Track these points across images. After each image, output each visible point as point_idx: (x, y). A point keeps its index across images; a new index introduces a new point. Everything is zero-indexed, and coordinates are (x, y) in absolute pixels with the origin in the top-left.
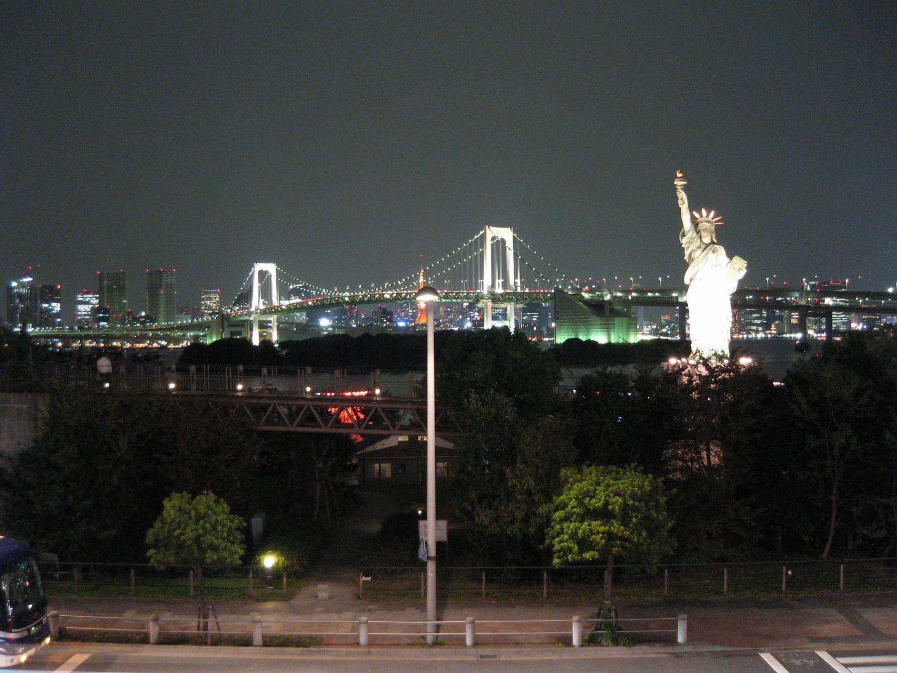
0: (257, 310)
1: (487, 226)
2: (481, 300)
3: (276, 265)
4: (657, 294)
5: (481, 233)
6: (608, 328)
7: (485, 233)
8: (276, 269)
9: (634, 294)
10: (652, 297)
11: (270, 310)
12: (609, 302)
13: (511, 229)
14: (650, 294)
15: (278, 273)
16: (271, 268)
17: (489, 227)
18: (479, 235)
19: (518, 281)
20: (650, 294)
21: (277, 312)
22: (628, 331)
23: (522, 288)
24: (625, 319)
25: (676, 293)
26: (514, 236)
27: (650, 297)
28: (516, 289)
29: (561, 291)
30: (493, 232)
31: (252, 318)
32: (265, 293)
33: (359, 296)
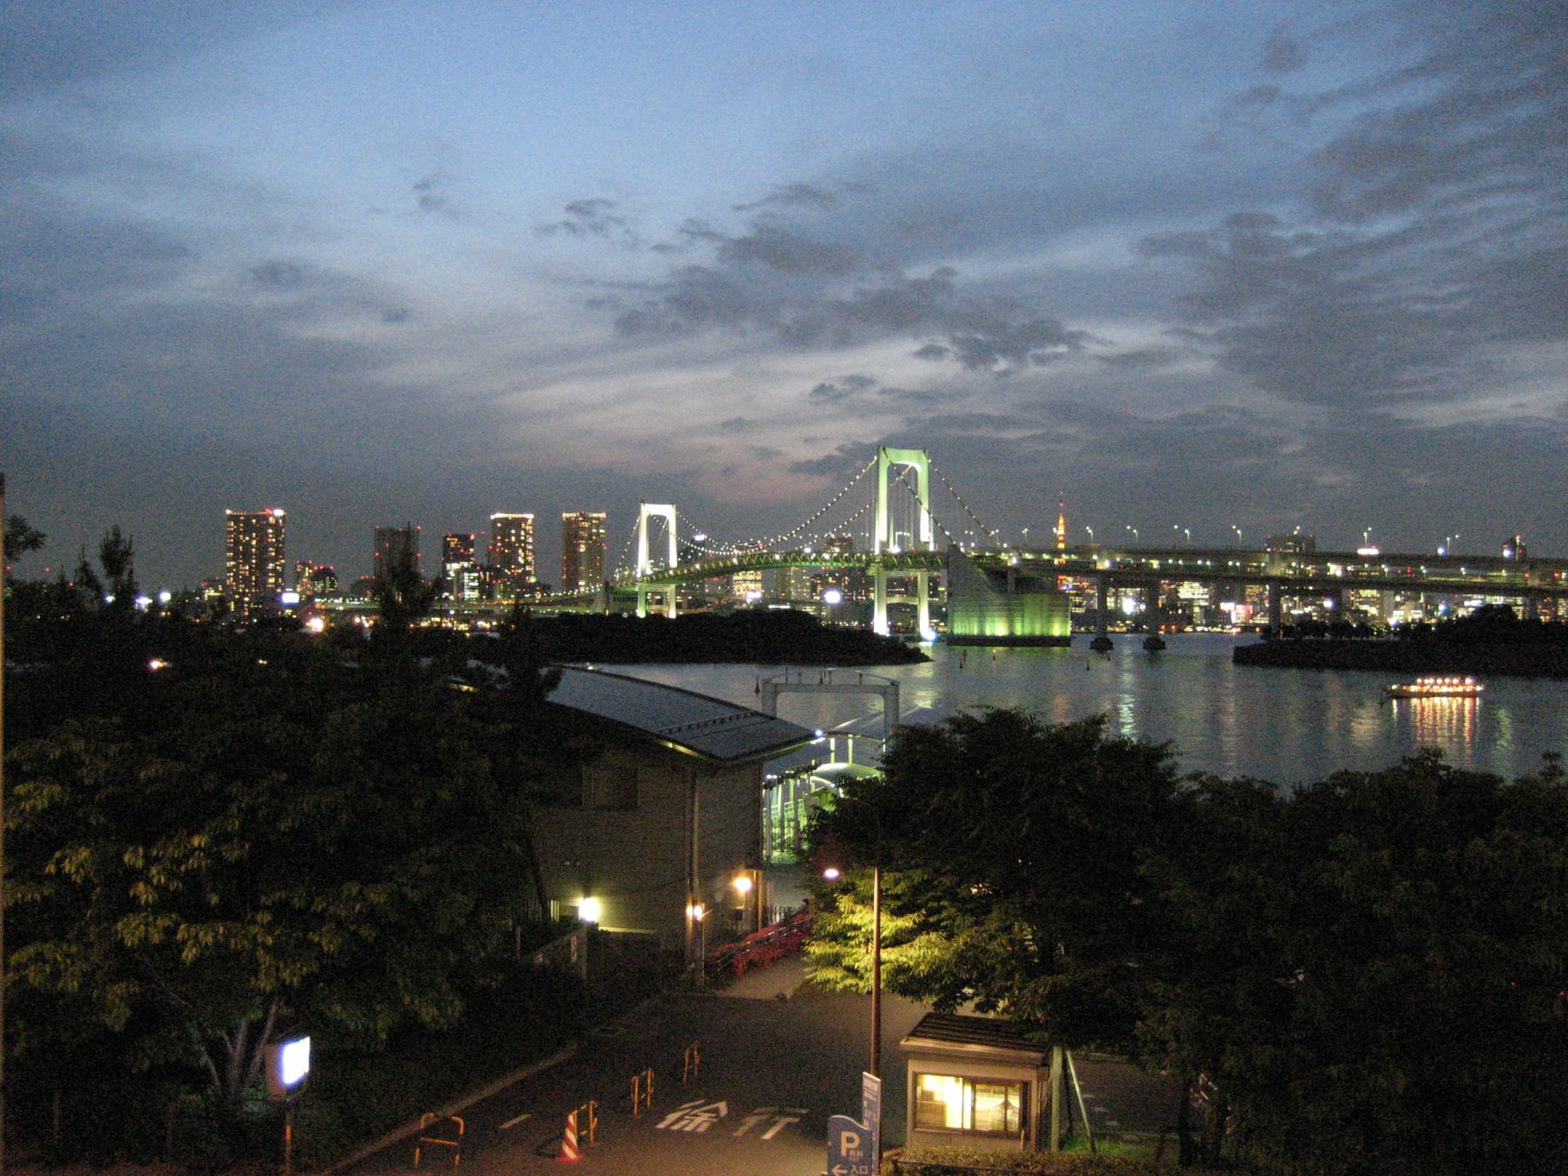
4: (1074, 557)
6: (1009, 610)
11: (660, 577)
15: (678, 520)
16: (668, 512)
22: (1051, 616)
24: (1046, 599)
31: (637, 589)
32: (658, 551)
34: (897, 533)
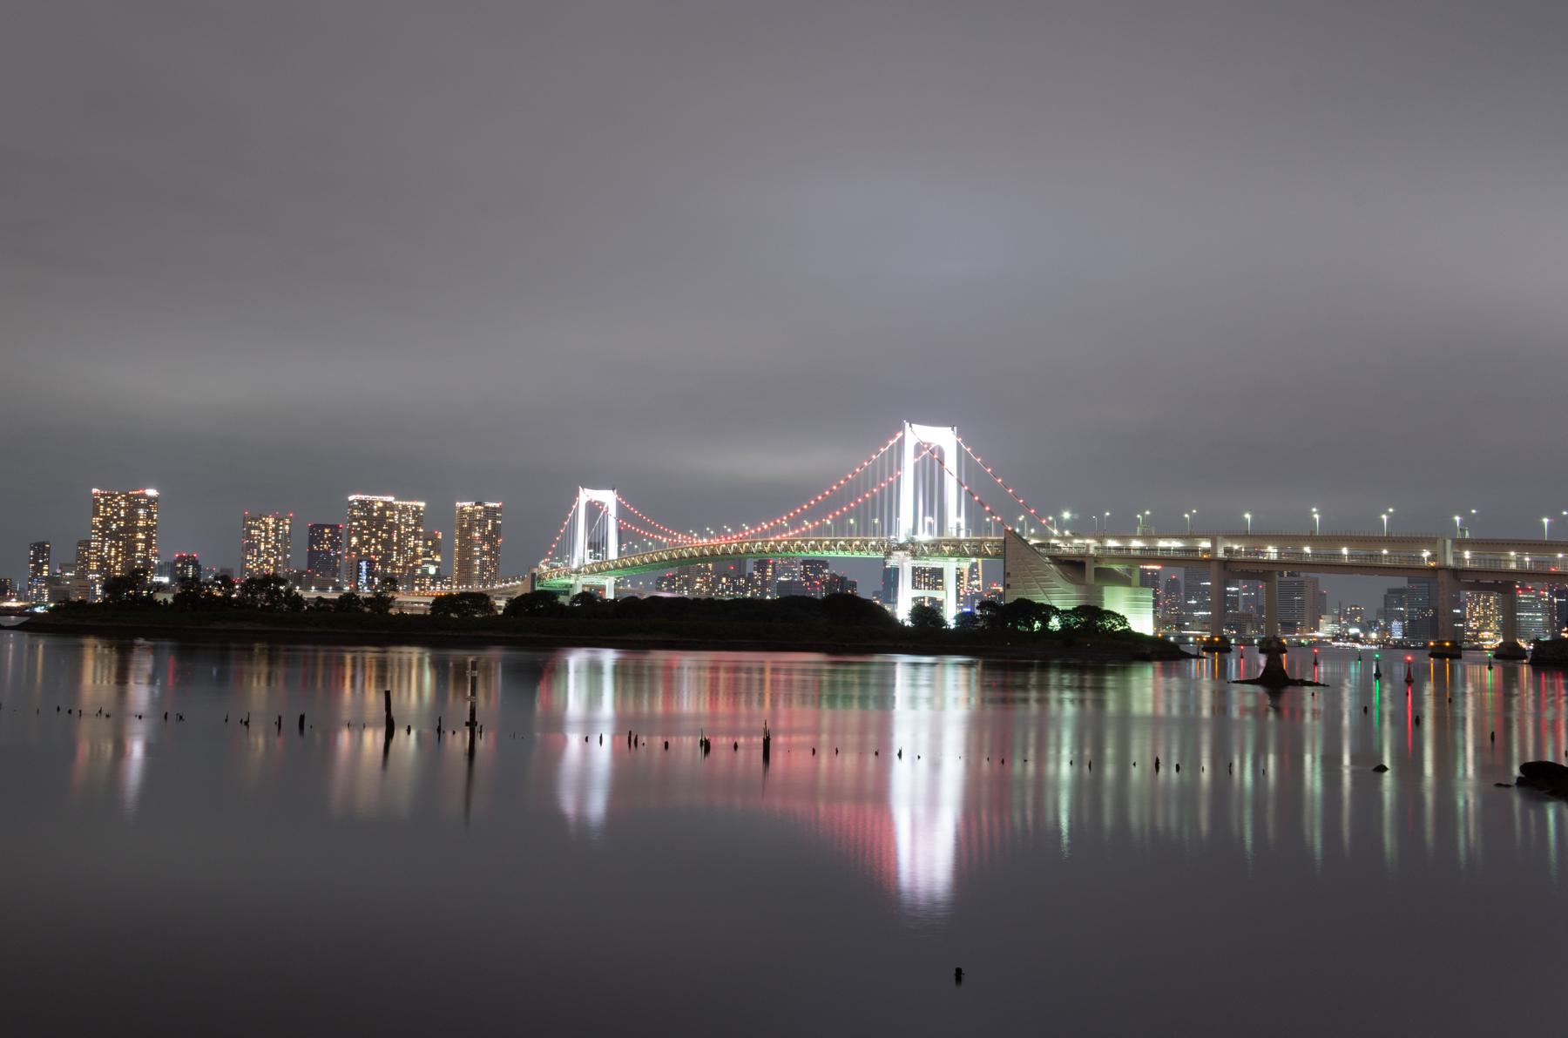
0: (580, 567)
1: (907, 424)
2: (895, 553)
5: (900, 435)
7: (903, 439)
12: (1096, 559)
13: (953, 429)
14: (1162, 544)
16: (608, 498)
17: (910, 426)
18: (895, 440)
19: (962, 521)
20: (1162, 544)
21: (616, 567)
23: (967, 533)
26: (958, 443)
28: (958, 534)
29: (1019, 537)
30: (916, 434)
33: (719, 545)
34: (928, 519)
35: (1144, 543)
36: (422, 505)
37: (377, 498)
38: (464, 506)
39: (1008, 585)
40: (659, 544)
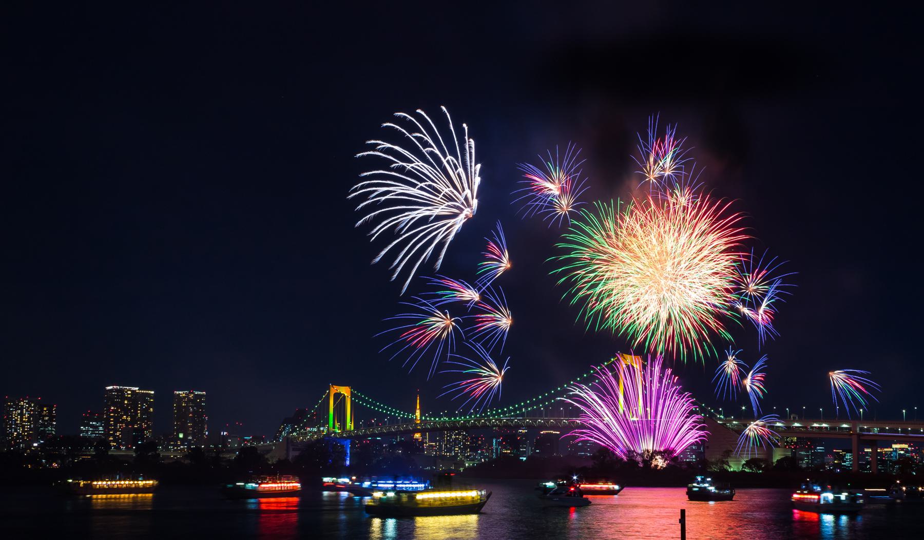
1: (621, 354)
3: (351, 389)
4: (824, 425)
8: (351, 392)
9: (796, 425)
10: (818, 427)
14: (815, 425)
20: (815, 425)
25: (846, 424)
27: (816, 427)
33: (460, 421)
35: (800, 424)
36: (153, 392)
37: (128, 388)
38: (179, 394)
39: (708, 447)
40: (394, 420)
